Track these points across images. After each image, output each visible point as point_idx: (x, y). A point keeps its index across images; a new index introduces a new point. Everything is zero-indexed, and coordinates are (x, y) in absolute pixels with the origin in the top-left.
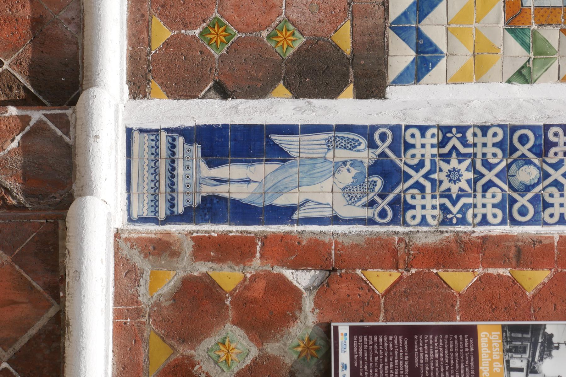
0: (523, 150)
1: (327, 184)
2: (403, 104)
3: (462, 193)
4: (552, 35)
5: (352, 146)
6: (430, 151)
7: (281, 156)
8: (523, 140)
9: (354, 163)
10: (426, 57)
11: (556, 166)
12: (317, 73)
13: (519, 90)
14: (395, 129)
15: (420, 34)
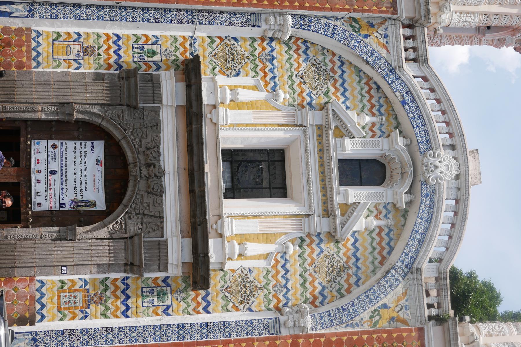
0: (59, 334)
1: (24, 342)
2: (39, 327)
3: (48, 343)
4: (66, 312)
5: (28, 335)
6: (42, 336)
8: (59, 332)
9: (28, 338)
10: (43, 317)
11: (65, 337)
13: (61, 322)
14: (36, 332)
15: (42, 313)
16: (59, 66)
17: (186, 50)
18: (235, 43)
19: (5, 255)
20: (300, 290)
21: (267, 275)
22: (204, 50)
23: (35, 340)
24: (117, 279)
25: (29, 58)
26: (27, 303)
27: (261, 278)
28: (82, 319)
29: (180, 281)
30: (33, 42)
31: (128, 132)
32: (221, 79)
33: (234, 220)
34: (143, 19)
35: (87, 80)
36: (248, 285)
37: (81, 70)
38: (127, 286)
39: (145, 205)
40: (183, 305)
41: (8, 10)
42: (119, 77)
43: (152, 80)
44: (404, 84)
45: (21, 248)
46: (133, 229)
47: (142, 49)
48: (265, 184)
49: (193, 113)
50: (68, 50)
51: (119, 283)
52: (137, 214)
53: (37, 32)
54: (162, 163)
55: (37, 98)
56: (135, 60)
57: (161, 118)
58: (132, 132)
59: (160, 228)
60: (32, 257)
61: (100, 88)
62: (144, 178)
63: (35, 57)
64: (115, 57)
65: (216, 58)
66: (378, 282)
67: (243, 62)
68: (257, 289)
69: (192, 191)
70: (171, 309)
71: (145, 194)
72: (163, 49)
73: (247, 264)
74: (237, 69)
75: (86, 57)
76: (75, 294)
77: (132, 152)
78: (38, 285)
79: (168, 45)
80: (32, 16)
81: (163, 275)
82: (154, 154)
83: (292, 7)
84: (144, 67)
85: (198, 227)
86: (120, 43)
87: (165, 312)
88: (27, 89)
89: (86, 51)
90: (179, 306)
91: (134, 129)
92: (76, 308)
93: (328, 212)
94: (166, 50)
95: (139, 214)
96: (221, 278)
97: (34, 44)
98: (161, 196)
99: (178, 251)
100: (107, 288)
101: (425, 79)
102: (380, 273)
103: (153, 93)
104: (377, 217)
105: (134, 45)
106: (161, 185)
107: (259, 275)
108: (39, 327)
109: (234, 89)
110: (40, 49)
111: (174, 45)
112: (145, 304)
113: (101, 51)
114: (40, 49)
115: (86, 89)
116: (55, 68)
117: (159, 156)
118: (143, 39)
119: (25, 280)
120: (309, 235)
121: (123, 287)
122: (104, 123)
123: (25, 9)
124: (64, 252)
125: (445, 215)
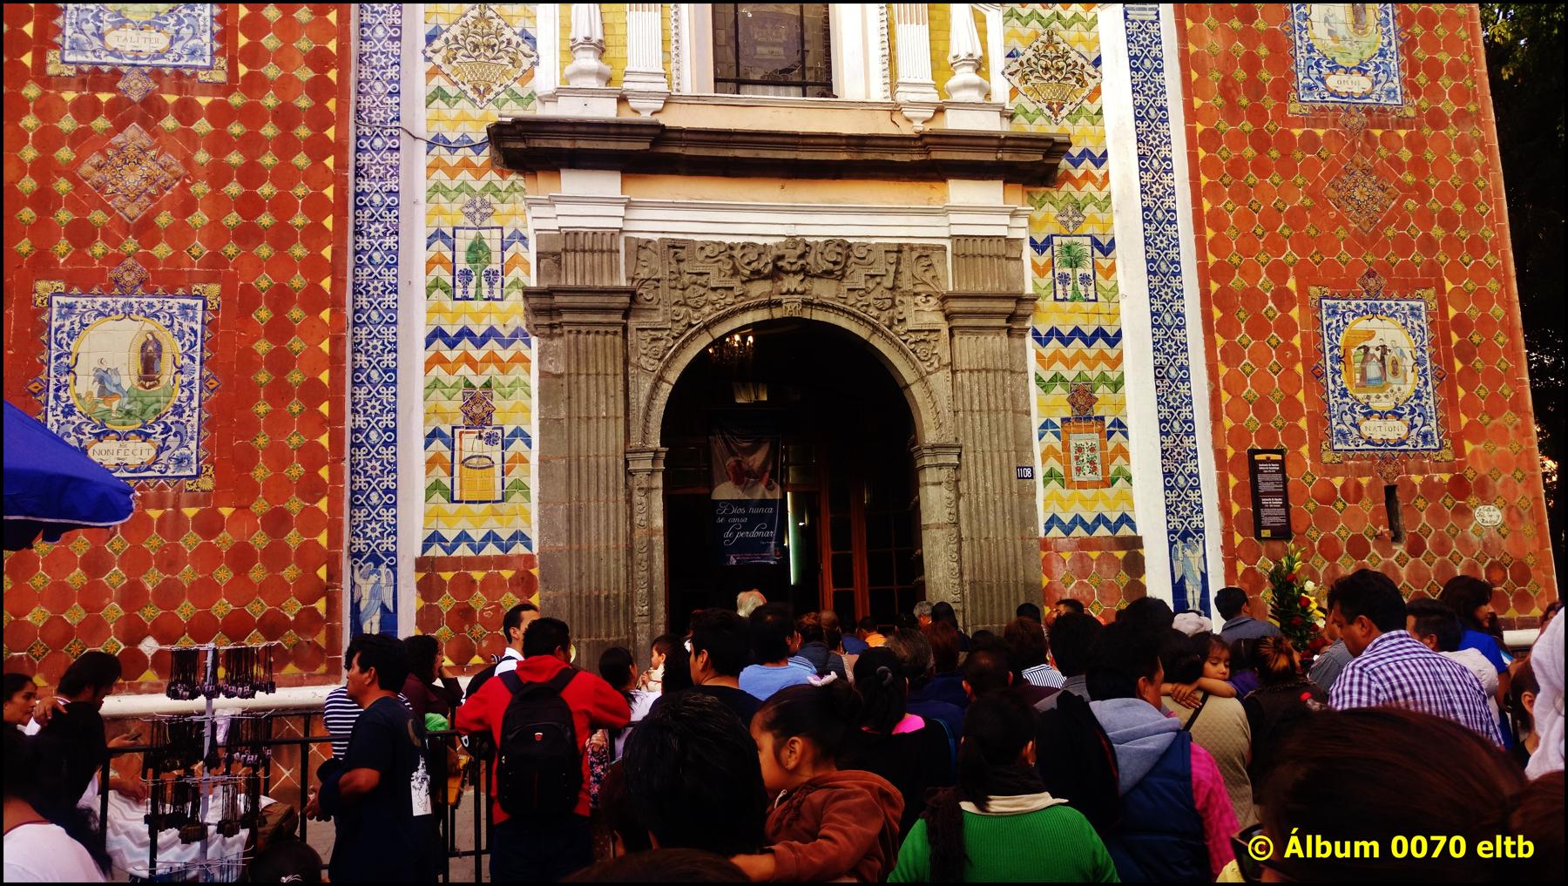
4: (1112, 469)
7: (1183, 579)
16: (522, 487)
17: (466, 164)
18: (444, 36)
19: (1000, 605)
21: (1019, 17)
22: (465, 118)
23: (1185, 535)
24: (1039, 356)
26: (1094, 554)
27: (1028, 31)
28: (1125, 434)
29: (1038, 215)
30: (456, 554)
31: (697, 318)
32: (546, 78)
33: (901, 80)
34: (388, 266)
35: (563, 414)
36: (1043, 63)
37: (534, 432)
38: (1054, 332)
39: (871, 285)
40: (1090, 210)
41: (376, 618)
42: (551, 337)
43: (554, 254)
45: (981, 570)
46: (930, 316)
47: (467, 274)
49: (647, 152)
51: (1048, 351)
52: (893, 306)
53: (427, 544)
54: (770, 241)
55: (616, 539)
56: (498, 295)
57: (656, 237)
58: (696, 309)
59: (927, 253)
60: (1002, 545)
61: (583, 386)
62: (807, 285)
63: (500, 547)
64: (492, 344)
65: (488, 89)
67: (495, 22)
68: (1050, 41)
70: (1100, 239)
71: (847, 284)
72: (462, 220)
73: (997, 61)
74: (515, 39)
75: (496, 420)
76: (1073, 450)
77: (745, 310)
78: (1056, 532)
80: (387, 553)
82: (753, 256)
84: (517, 272)
85: (926, 160)
86: (452, 331)
87: (1107, 249)
88: (593, 563)
90: (1095, 221)
91: (685, 304)
92: (1103, 447)
94: (467, 214)
95: (893, 300)
96: (1031, 122)
97: (463, 551)
98: (850, 246)
100: (1058, 378)
103: (592, 251)
105: (459, 294)
106: (827, 244)
107: (1020, 37)
109: (571, 49)
110: (477, 536)
111: (453, 194)
112: (1092, 297)
113: (478, 381)
114: (477, 536)
115: (589, 418)
116: (527, 496)
117: (754, 245)
119: (1046, 560)
121: (1055, 343)
122: (673, 376)
123: (371, 573)
124: (989, 472)
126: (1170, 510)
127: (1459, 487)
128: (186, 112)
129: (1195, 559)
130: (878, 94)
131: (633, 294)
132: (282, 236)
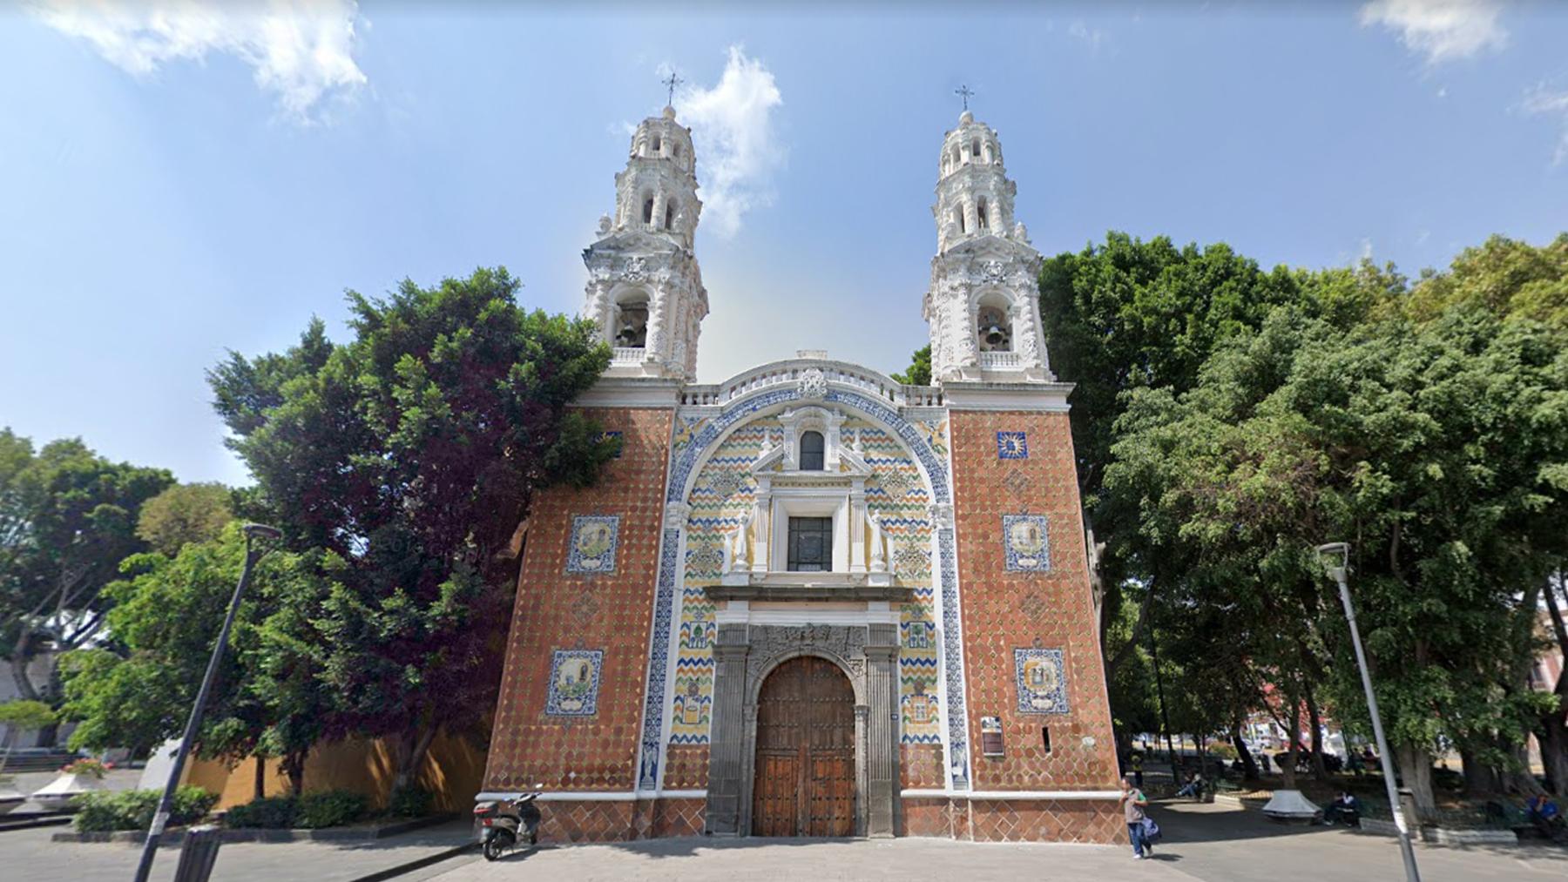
2: (945, 741)
10: (935, 737)
12: (940, 756)
16: (706, 718)
20: (914, 511)
25: (698, 747)
32: (725, 569)
44: (738, 408)
48: (819, 535)
49: (757, 594)
50: (692, 710)
59: (860, 629)
66: (909, 444)
69: (827, 600)
79: (691, 617)
81: (899, 628)
83: (661, 500)
85: (859, 595)
89: (693, 691)
93: (847, 482)
97: (684, 742)
99: (879, 614)
101: (733, 389)
102: (900, 442)
104: (852, 441)
108: (945, 741)
118: (685, 639)
120: (867, 500)
125: (853, 384)
126: (952, 735)
127: (1076, 728)
128: (604, 586)
129: (962, 756)
130: (845, 570)
131: (750, 648)
132: (630, 628)
